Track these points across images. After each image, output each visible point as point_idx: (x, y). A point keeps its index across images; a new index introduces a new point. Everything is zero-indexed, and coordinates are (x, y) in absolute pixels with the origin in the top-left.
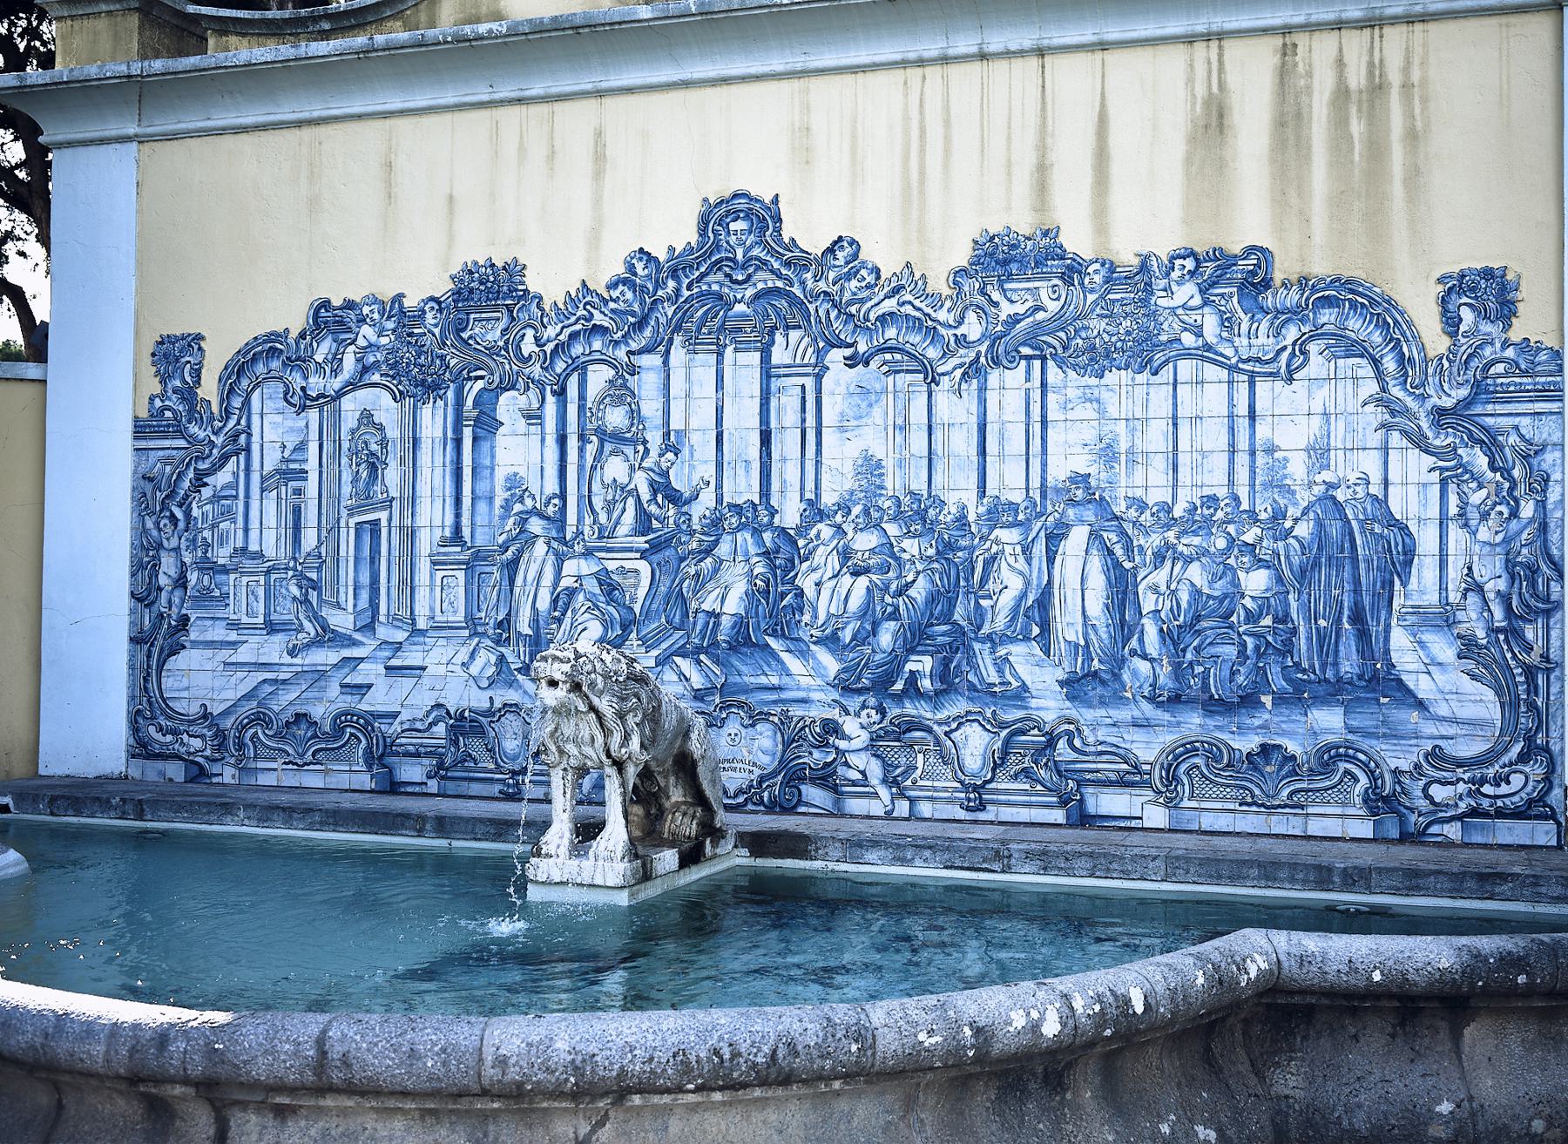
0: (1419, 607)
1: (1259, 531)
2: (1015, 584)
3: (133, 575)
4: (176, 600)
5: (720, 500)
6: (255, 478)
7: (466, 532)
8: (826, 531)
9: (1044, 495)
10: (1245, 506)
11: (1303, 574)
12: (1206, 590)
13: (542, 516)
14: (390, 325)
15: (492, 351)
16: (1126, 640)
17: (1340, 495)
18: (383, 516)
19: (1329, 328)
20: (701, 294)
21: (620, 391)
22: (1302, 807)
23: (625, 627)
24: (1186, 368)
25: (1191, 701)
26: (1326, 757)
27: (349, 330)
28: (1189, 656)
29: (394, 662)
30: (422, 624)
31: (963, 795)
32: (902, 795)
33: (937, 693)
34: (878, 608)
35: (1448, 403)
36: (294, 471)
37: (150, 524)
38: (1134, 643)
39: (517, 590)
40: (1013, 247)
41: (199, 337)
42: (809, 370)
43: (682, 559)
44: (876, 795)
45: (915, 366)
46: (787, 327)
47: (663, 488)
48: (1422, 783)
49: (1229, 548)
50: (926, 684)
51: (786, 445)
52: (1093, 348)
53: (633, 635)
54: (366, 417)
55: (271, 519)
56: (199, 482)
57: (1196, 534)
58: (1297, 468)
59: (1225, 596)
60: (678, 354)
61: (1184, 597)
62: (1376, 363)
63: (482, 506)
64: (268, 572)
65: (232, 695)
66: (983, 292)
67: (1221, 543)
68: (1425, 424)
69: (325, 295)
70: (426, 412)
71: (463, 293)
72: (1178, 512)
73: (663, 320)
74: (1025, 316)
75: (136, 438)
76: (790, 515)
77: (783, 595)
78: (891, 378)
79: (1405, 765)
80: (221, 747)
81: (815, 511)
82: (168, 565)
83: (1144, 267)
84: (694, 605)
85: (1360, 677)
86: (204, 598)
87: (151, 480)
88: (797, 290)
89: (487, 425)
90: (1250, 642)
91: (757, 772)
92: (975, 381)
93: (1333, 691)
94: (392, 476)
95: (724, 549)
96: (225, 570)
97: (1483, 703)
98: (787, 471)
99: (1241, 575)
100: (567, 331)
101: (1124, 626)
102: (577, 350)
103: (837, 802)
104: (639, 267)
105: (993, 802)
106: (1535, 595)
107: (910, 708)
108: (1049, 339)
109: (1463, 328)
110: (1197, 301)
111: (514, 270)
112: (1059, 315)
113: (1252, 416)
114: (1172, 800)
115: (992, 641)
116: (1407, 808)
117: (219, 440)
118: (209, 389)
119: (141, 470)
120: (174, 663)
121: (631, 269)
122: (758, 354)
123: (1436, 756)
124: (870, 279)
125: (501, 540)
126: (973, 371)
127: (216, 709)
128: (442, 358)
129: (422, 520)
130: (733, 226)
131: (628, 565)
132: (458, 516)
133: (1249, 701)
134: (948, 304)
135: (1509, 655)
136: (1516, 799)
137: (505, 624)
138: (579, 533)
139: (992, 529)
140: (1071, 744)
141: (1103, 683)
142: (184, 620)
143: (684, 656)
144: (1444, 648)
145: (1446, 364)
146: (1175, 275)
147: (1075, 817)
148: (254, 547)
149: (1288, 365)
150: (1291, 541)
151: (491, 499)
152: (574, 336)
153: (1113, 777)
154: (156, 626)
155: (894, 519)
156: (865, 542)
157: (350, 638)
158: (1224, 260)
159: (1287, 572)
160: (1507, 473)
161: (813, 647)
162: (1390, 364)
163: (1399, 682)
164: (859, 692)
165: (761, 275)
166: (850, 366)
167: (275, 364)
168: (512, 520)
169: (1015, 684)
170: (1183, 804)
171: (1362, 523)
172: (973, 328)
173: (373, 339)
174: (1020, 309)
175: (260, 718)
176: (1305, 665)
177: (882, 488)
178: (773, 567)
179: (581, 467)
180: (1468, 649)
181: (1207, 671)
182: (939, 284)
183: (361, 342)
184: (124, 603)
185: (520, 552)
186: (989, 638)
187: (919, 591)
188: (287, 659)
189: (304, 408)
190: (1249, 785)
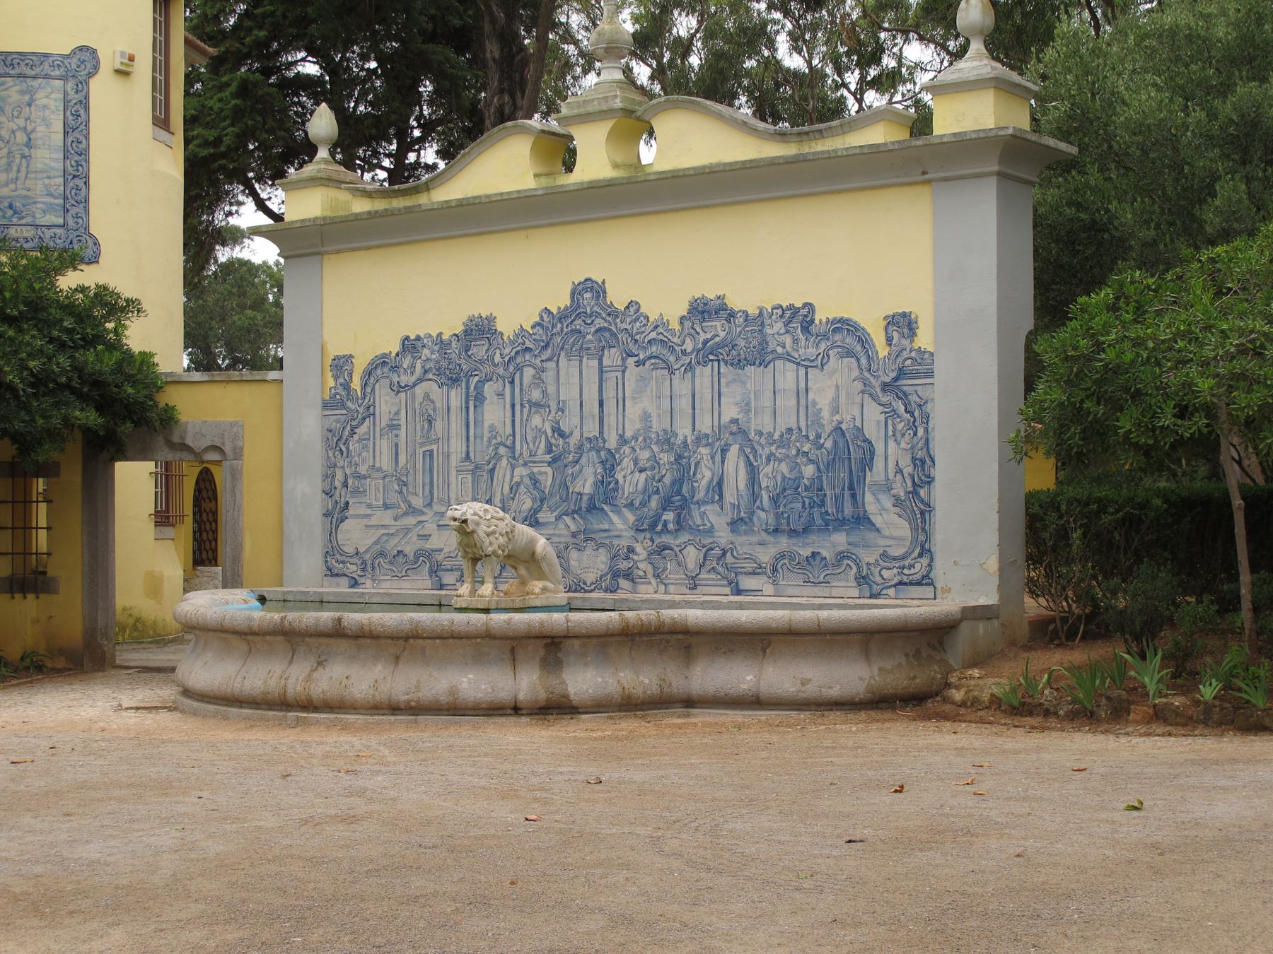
2: (708, 474)
3: (324, 481)
4: (343, 494)
5: (582, 436)
6: (378, 429)
7: (472, 455)
8: (626, 449)
10: (804, 433)
11: (829, 465)
13: (505, 445)
14: (436, 348)
15: (481, 362)
16: (755, 501)
17: (844, 429)
18: (435, 447)
19: (839, 343)
20: (572, 331)
21: (538, 380)
23: (542, 501)
24: (779, 363)
25: (783, 531)
27: (418, 351)
28: (781, 509)
29: (441, 523)
32: (661, 582)
33: (676, 531)
35: (888, 380)
36: (395, 425)
37: (331, 455)
38: (758, 503)
39: (494, 484)
40: (706, 304)
41: (351, 356)
43: (566, 466)
44: (650, 583)
45: (664, 365)
46: (610, 347)
50: (671, 526)
51: (610, 406)
52: (739, 355)
54: (427, 396)
55: (385, 450)
56: (353, 433)
57: (783, 447)
58: (826, 414)
59: (796, 478)
60: (563, 362)
61: (779, 479)
62: (858, 360)
63: (478, 441)
64: (384, 478)
65: (369, 542)
66: (693, 328)
67: (794, 452)
68: (878, 390)
69: (407, 334)
70: (453, 393)
71: (467, 332)
74: (712, 339)
75: (324, 410)
76: (612, 442)
77: (610, 483)
79: (872, 561)
80: (364, 570)
81: (623, 440)
82: (339, 476)
83: (761, 314)
84: (571, 490)
85: (853, 517)
86: (356, 492)
87: (330, 431)
88: (613, 328)
89: (480, 399)
90: (807, 503)
91: (600, 573)
93: (841, 523)
94: (439, 425)
95: (584, 460)
96: (365, 478)
97: (902, 529)
98: (611, 420)
99: (803, 467)
100: (514, 351)
101: (754, 496)
102: (519, 360)
103: (634, 588)
104: (545, 317)
105: (700, 585)
106: (926, 476)
107: (666, 539)
109: (894, 342)
110: (783, 331)
111: (491, 319)
112: (724, 339)
113: (807, 390)
117: (361, 410)
118: (356, 384)
119: (327, 426)
120: (344, 526)
121: (541, 317)
122: (597, 361)
123: (884, 555)
124: (644, 322)
125: (487, 458)
126: (690, 368)
127: (361, 550)
128: (459, 365)
129: (452, 449)
130: (585, 296)
131: (543, 470)
132: (468, 447)
133: (806, 530)
134: (678, 334)
138: (521, 454)
139: (698, 446)
140: (732, 553)
141: (746, 523)
142: (347, 504)
143: (567, 515)
144: (887, 502)
146: (774, 317)
147: (735, 591)
148: (377, 465)
151: (482, 437)
152: (517, 353)
153: (750, 570)
154: (335, 508)
155: (656, 443)
156: (644, 455)
157: (421, 511)
158: (794, 310)
159: (822, 466)
160: (912, 414)
161: (623, 509)
162: (864, 361)
164: (643, 531)
165: (598, 321)
167: (386, 369)
168: (491, 449)
169: (709, 525)
172: (689, 346)
173: (429, 355)
174: (709, 336)
175: (382, 554)
176: (830, 511)
178: (605, 470)
179: (521, 420)
180: (897, 502)
182: (675, 325)
183: (423, 358)
184: (320, 496)
185: (496, 464)
186: (698, 502)
187: (667, 480)
188: (393, 523)
189: (399, 392)
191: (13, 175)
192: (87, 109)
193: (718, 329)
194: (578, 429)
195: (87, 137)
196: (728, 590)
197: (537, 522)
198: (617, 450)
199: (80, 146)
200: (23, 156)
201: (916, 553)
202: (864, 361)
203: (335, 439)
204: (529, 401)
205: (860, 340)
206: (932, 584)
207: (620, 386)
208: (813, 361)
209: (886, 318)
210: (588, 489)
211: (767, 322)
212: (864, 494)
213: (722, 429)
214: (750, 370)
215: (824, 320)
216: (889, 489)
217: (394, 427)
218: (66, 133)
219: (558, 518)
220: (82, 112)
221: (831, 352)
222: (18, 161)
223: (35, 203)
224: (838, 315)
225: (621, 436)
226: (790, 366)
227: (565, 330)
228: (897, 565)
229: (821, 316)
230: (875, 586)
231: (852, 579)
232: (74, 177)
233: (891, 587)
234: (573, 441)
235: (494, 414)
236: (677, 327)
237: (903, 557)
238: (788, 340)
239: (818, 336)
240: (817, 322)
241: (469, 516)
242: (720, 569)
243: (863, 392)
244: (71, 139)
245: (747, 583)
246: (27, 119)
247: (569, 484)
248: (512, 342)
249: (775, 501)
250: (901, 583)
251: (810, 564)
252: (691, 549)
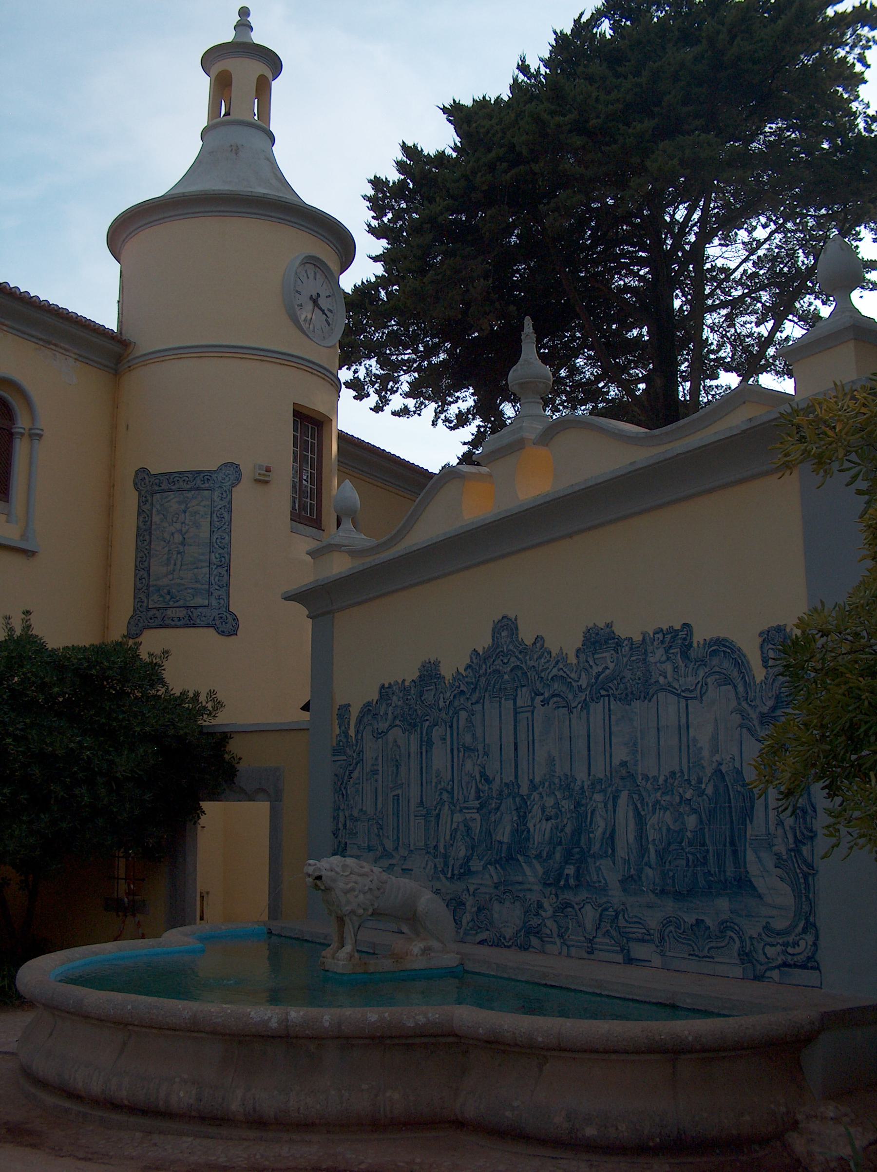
0: (757, 836)
1: (692, 791)
2: (602, 824)
5: (501, 782)
7: (424, 800)
8: (535, 795)
9: (611, 775)
12: (672, 828)
16: (643, 857)
17: (724, 769)
18: (399, 792)
19: (717, 669)
20: (494, 671)
22: (713, 958)
23: (473, 849)
24: (661, 695)
26: (722, 927)
28: (667, 867)
29: (404, 867)
30: (412, 848)
31: (585, 944)
33: (576, 886)
34: (555, 839)
35: (765, 709)
38: (646, 859)
40: (597, 634)
41: (349, 705)
42: (528, 709)
43: (490, 813)
45: (564, 703)
47: (483, 774)
48: (762, 945)
49: (680, 803)
50: (572, 882)
52: (626, 689)
53: (475, 854)
58: (706, 753)
62: (735, 687)
67: (677, 799)
68: (756, 722)
72: (661, 781)
73: (482, 686)
74: (603, 672)
78: (556, 711)
81: (533, 787)
82: (342, 819)
83: (644, 640)
88: (523, 666)
89: (430, 743)
92: (585, 711)
95: (503, 808)
99: (685, 817)
101: (643, 850)
102: (456, 703)
104: (474, 657)
107: (568, 896)
108: (610, 685)
110: (664, 658)
114: (662, 951)
115: (594, 857)
116: (756, 960)
118: (352, 732)
123: (767, 928)
126: (585, 705)
128: (416, 710)
135: (796, 865)
136: (802, 956)
137: (436, 847)
139: (593, 793)
140: (624, 915)
141: (635, 881)
143: (491, 864)
144: (770, 862)
145: (763, 684)
146: (656, 643)
149: (701, 692)
150: (705, 797)
154: (338, 846)
156: (550, 802)
159: (704, 816)
162: (741, 688)
163: (750, 881)
164: (549, 885)
166: (543, 705)
170: (668, 954)
171: (732, 785)
172: (584, 683)
177: (555, 772)
178: (519, 817)
179: (458, 764)
180: (780, 862)
181: (674, 876)
182: (572, 660)
183: (393, 705)
185: (440, 810)
186: (593, 856)
187: (568, 830)
190: (694, 945)
191: (171, 568)
192: (230, 511)
193: (607, 659)
194: (499, 774)
196: (619, 958)
197: (469, 870)
198: (529, 796)
199: (223, 541)
200: (179, 553)
201: (799, 929)
202: (741, 688)
203: (339, 783)
204: (464, 745)
205: (737, 664)
206: (818, 968)
207: (530, 728)
208: (691, 691)
209: (760, 635)
210: (506, 839)
211: (650, 649)
212: (745, 850)
213: (614, 774)
214: (637, 704)
215: (702, 642)
216: (771, 845)
217: (375, 772)
218: (212, 532)
219: (485, 867)
220: (226, 515)
221: (709, 680)
223: (186, 589)
224: (714, 635)
225: (531, 781)
226: (672, 699)
227: (489, 671)
228: (781, 941)
229: (698, 637)
230: (759, 967)
231: (736, 955)
232: (218, 566)
233: (775, 967)
234: (496, 786)
235: (440, 758)
236: (575, 661)
237: (786, 932)
238: (668, 667)
239: (696, 661)
240: (695, 645)
241: (323, 873)
242: (614, 933)
243: (741, 726)
244: (216, 536)
245: (639, 951)
246: (182, 523)
247: (492, 831)
248: (452, 686)
249: (660, 855)
250: (785, 964)
251: (695, 934)
252: (588, 907)
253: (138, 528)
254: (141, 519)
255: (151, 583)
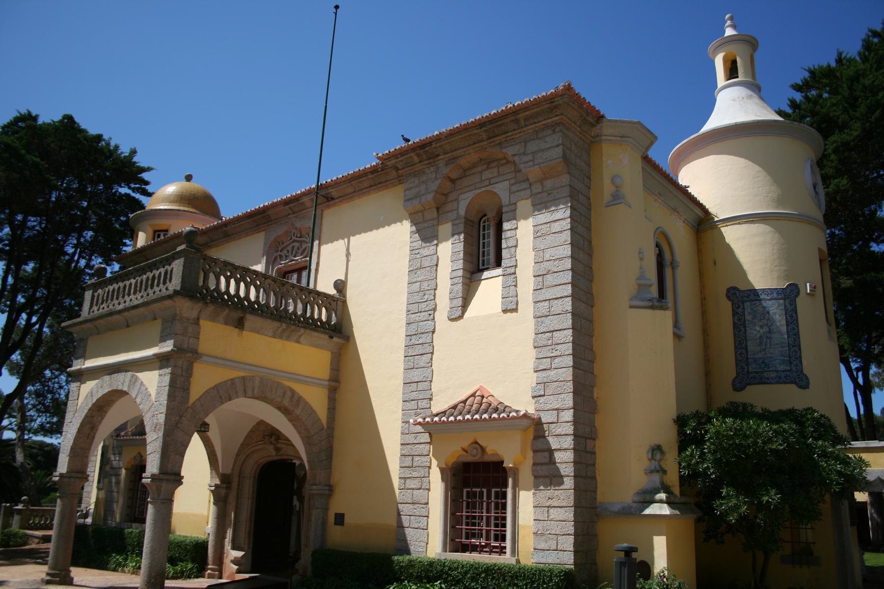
191: (763, 347)
195: (798, 326)
200: (767, 338)
220: (794, 315)
222: (765, 340)
223: (776, 360)
232: (793, 346)
244: (790, 328)
253: (734, 323)
254: (736, 317)
255: (749, 357)
